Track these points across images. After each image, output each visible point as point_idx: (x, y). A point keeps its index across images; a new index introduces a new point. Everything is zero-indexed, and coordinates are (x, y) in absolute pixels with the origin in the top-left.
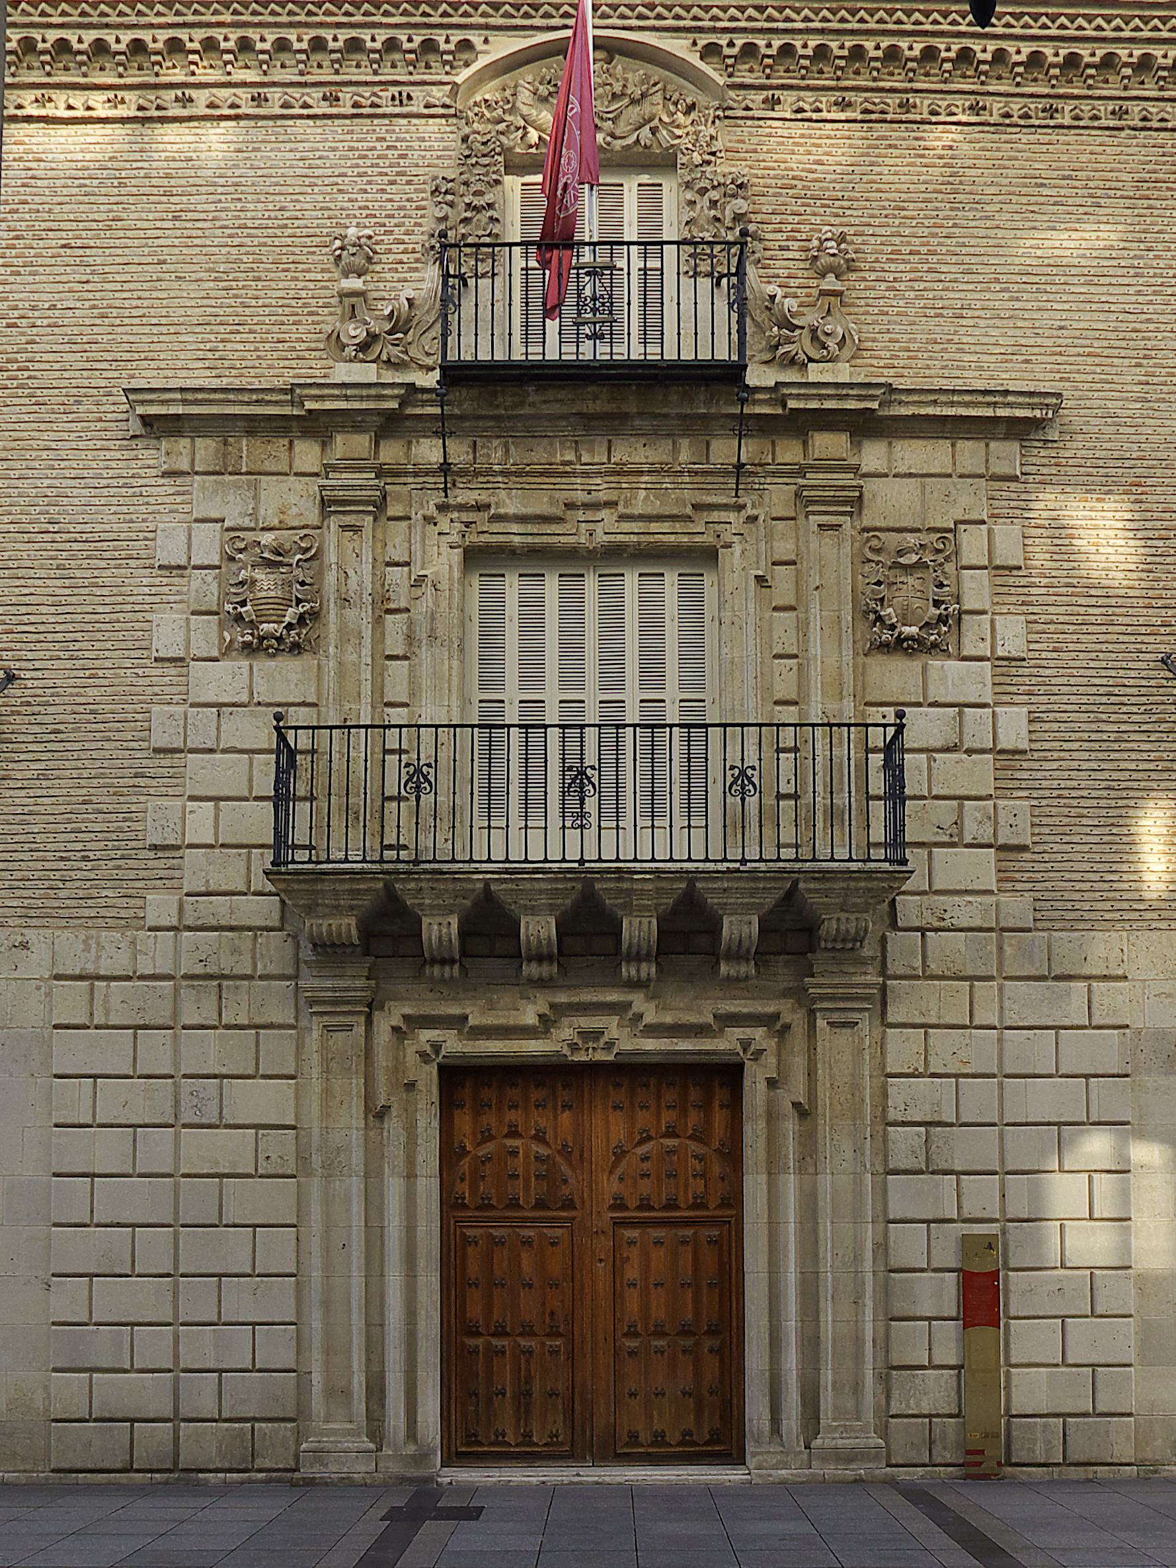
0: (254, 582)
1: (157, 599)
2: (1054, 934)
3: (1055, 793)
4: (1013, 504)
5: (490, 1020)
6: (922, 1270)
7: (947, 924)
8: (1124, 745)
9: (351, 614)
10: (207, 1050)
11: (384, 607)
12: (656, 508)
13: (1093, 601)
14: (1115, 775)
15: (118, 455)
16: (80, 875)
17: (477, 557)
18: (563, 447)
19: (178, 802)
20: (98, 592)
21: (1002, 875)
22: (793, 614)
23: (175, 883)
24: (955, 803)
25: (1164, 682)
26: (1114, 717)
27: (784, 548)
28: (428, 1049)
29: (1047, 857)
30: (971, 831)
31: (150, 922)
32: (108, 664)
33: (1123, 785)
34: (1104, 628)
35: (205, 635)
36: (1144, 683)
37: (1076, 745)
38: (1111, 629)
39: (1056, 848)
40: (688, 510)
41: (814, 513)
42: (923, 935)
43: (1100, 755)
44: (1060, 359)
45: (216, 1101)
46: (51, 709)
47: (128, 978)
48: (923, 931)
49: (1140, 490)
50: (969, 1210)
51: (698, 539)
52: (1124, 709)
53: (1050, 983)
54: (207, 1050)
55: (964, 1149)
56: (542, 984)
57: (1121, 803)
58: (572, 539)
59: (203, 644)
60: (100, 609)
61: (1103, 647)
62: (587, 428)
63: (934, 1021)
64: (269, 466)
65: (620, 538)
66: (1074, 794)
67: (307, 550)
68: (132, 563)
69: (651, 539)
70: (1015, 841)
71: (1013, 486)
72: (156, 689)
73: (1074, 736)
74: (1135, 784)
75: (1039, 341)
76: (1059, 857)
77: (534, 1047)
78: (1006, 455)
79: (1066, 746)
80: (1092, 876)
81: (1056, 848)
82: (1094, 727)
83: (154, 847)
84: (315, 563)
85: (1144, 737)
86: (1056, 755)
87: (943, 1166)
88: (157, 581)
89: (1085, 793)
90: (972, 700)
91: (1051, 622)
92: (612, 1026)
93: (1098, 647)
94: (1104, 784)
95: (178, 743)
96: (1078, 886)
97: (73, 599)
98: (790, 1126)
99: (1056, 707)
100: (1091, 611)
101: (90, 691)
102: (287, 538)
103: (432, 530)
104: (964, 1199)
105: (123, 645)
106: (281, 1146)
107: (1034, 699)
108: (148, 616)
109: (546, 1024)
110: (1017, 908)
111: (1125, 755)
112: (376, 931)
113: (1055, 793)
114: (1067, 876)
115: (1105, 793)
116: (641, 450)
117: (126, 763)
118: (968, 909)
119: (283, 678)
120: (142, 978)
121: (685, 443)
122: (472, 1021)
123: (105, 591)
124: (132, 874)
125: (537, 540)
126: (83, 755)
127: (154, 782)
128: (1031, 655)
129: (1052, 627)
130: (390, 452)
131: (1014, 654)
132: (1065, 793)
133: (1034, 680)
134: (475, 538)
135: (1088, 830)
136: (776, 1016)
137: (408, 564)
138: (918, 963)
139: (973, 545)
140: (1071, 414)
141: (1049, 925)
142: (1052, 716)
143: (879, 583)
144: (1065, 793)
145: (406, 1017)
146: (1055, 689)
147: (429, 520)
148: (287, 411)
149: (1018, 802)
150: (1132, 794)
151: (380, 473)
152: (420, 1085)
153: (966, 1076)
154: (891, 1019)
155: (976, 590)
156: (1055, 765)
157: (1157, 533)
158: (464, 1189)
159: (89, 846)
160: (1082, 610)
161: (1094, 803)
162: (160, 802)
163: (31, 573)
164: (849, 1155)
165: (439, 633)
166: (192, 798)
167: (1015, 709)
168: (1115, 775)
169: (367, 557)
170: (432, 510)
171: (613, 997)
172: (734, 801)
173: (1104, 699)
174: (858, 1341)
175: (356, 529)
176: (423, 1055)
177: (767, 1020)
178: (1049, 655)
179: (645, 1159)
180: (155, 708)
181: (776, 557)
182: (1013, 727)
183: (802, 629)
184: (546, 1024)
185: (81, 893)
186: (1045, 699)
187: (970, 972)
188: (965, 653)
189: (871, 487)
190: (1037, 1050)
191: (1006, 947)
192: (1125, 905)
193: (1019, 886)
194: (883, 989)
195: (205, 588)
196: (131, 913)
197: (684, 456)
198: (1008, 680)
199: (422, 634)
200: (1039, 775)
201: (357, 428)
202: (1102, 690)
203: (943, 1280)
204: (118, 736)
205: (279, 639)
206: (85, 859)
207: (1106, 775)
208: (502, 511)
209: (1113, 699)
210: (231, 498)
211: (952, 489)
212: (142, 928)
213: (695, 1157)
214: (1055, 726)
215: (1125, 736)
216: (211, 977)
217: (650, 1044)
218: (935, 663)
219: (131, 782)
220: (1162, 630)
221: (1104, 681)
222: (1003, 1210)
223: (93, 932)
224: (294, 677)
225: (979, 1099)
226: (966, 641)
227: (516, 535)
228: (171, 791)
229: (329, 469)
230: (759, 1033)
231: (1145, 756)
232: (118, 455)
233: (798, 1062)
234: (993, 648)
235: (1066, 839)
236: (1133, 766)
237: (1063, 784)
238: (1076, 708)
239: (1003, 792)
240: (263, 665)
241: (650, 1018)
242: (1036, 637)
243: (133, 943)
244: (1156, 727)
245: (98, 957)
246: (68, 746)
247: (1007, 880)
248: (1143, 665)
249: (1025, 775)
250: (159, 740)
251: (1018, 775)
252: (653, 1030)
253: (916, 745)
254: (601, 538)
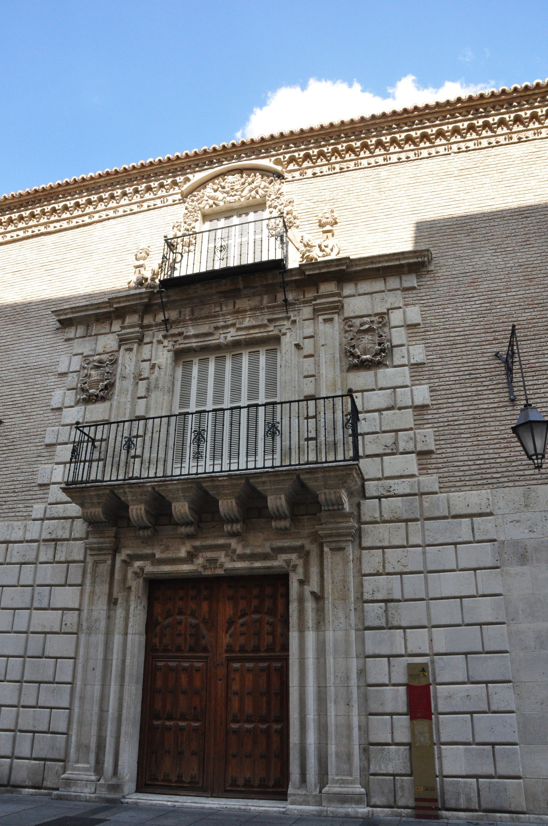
1: (56, 387)
2: (450, 494)
3: (446, 424)
4: (414, 299)
6: (386, 685)
7: (392, 493)
8: (480, 397)
9: (125, 383)
10: (47, 574)
11: (138, 378)
12: (254, 323)
13: (457, 334)
14: (478, 412)
15: (51, 336)
16: (11, 499)
17: (181, 356)
18: (215, 307)
19: (51, 466)
20: (36, 386)
21: (421, 467)
22: (312, 359)
23: (46, 500)
24: (393, 434)
25: (498, 365)
26: (473, 385)
27: (309, 331)
28: (138, 571)
29: (444, 455)
30: (402, 446)
31: (33, 517)
32: (35, 413)
33: (482, 416)
34: (464, 345)
36: (487, 367)
37: (455, 400)
38: (467, 345)
39: (449, 450)
40: (266, 322)
41: (321, 315)
42: (380, 500)
43: (468, 403)
44: (432, 239)
45: (48, 597)
46: (12, 433)
47: (21, 542)
48: (379, 498)
49: (475, 284)
50: (412, 649)
51: (271, 333)
52: (479, 380)
53: (450, 520)
54: (47, 574)
55: (406, 614)
56: (190, 537)
57: (481, 425)
58: (217, 341)
59: (69, 401)
60: (36, 393)
61: (465, 353)
62: (225, 297)
63: (386, 544)
64: (102, 331)
65: (237, 338)
66: (456, 423)
67: (112, 360)
68: (49, 374)
69: (251, 336)
70: (425, 448)
71: (414, 292)
72: (50, 421)
73: (453, 396)
74: (488, 415)
75: (422, 234)
76: (450, 455)
77: (185, 568)
78: (411, 281)
79: (450, 401)
80: (470, 463)
81: (449, 450)
82: (464, 390)
83: (40, 485)
84: (115, 366)
85: (490, 392)
86: (445, 405)
87: (395, 624)
88: (56, 380)
89: (462, 422)
90: (400, 384)
91: (438, 346)
92: (222, 557)
93: (462, 353)
94: (471, 417)
95: (54, 441)
96: (462, 468)
97: (27, 391)
98: (310, 605)
99: (443, 383)
100: (457, 338)
101: (27, 425)
102: (104, 357)
103: (161, 346)
104: (408, 643)
105: (41, 405)
106: (72, 618)
107: (432, 381)
108: (52, 393)
109: (191, 557)
110: (430, 482)
111: (481, 402)
112: (116, 515)
113: (446, 424)
114: (456, 464)
115: (472, 421)
116: (247, 303)
117: (35, 452)
118: (403, 485)
119: (97, 411)
120: (28, 541)
121: (266, 297)
122: (157, 556)
123: (38, 386)
124: (30, 497)
125: (202, 344)
126: (20, 450)
127: (44, 459)
128: (429, 361)
129: (438, 348)
130: (148, 320)
131: (419, 361)
132: (452, 423)
133: (431, 372)
134: (177, 347)
135: (465, 440)
136: (302, 547)
137: (150, 360)
138: (377, 515)
139: (396, 318)
141: (448, 489)
142: (441, 388)
143: (352, 339)
144: (452, 423)
145: (128, 555)
146: (442, 375)
147: (160, 342)
149: (426, 430)
150: (487, 420)
151: (142, 327)
152: (133, 589)
153: (406, 573)
154: (364, 544)
155: (398, 336)
156: (445, 410)
157: (486, 301)
158: (156, 641)
159: (17, 486)
160: (452, 338)
161: (467, 426)
162: (43, 466)
163: (14, 383)
164: (342, 620)
165: (160, 386)
166: (57, 463)
167: (422, 386)
168: (478, 412)
169: (134, 359)
170: (160, 338)
171: (221, 541)
172: (269, 439)
173: (467, 377)
174: (349, 727)
175: (131, 350)
176: (135, 573)
177: (299, 550)
178: (438, 360)
179: (242, 625)
180: (48, 428)
181: (305, 335)
182: (422, 394)
183: (317, 365)
184: (191, 557)
185: (11, 506)
186: (437, 380)
187: (405, 517)
188: (395, 364)
189: (346, 301)
190: (446, 557)
191: (424, 503)
192: (489, 476)
193: (430, 471)
194: (359, 530)
195: (72, 380)
196: (27, 514)
197: (265, 301)
198: (418, 374)
199: (152, 386)
200: (437, 416)
201: (135, 312)
202: (466, 373)
203: (398, 690)
204: (34, 441)
205: (97, 396)
206: (14, 492)
207: (472, 412)
208: (188, 334)
209: (472, 376)
210: (87, 345)
211: (385, 296)
212: (29, 520)
213: (268, 623)
214: (443, 392)
215: (480, 393)
216: (53, 540)
217: (239, 565)
218: (381, 371)
219: (35, 459)
220: (494, 342)
221: (467, 368)
222: (431, 648)
223: (12, 523)
224: (101, 410)
225: (414, 585)
226: (395, 359)
227: (194, 343)
228: (49, 461)
229: (123, 328)
231: (492, 401)
232: (51, 336)
233: (314, 570)
234: (409, 360)
235: (453, 445)
236: (486, 406)
237: (450, 419)
238: (453, 382)
239: (418, 426)
240: (90, 407)
241: (239, 551)
242: (430, 353)
243: (25, 526)
244: (496, 386)
245: (11, 533)
246: (16, 447)
247: (423, 469)
248: (486, 359)
249: (430, 417)
250: (48, 441)
251: (426, 417)
252: (242, 557)
253: (372, 409)
254: (229, 338)
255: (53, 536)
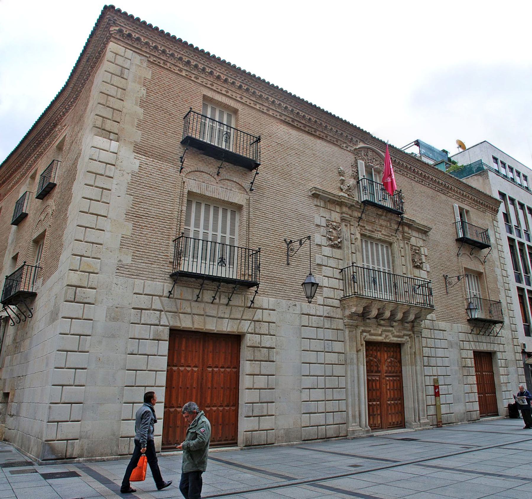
0: (332, 232)
5: (375, 332)
10: (329, 334)
35: (324, 241)
54: (329, 334)
55: (433, 362)
120: (317, 316)
122: (372, 332)
140: (430, 233)
148: (337, 199)
166: (324, 276)
217: (395, 339)
230: (408, 337)
241: (396, 333)
255: (329, 315)
